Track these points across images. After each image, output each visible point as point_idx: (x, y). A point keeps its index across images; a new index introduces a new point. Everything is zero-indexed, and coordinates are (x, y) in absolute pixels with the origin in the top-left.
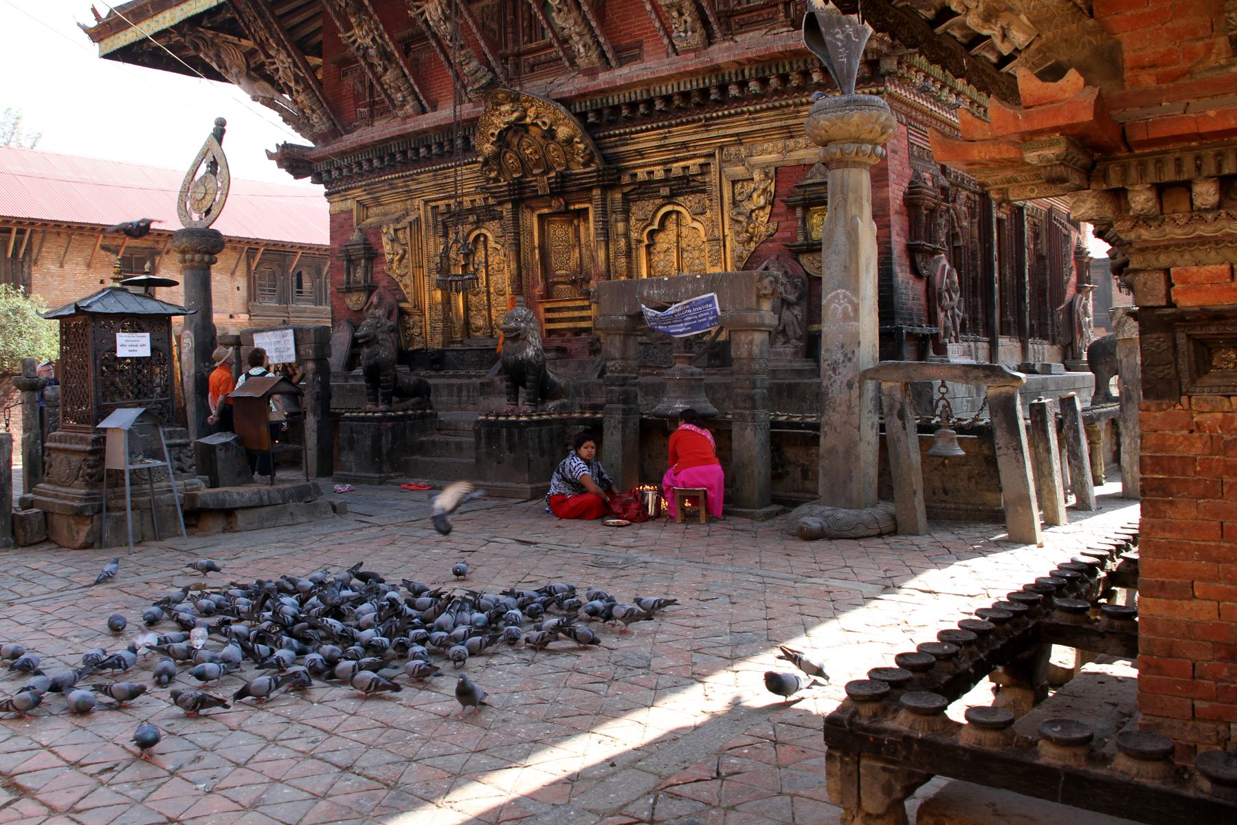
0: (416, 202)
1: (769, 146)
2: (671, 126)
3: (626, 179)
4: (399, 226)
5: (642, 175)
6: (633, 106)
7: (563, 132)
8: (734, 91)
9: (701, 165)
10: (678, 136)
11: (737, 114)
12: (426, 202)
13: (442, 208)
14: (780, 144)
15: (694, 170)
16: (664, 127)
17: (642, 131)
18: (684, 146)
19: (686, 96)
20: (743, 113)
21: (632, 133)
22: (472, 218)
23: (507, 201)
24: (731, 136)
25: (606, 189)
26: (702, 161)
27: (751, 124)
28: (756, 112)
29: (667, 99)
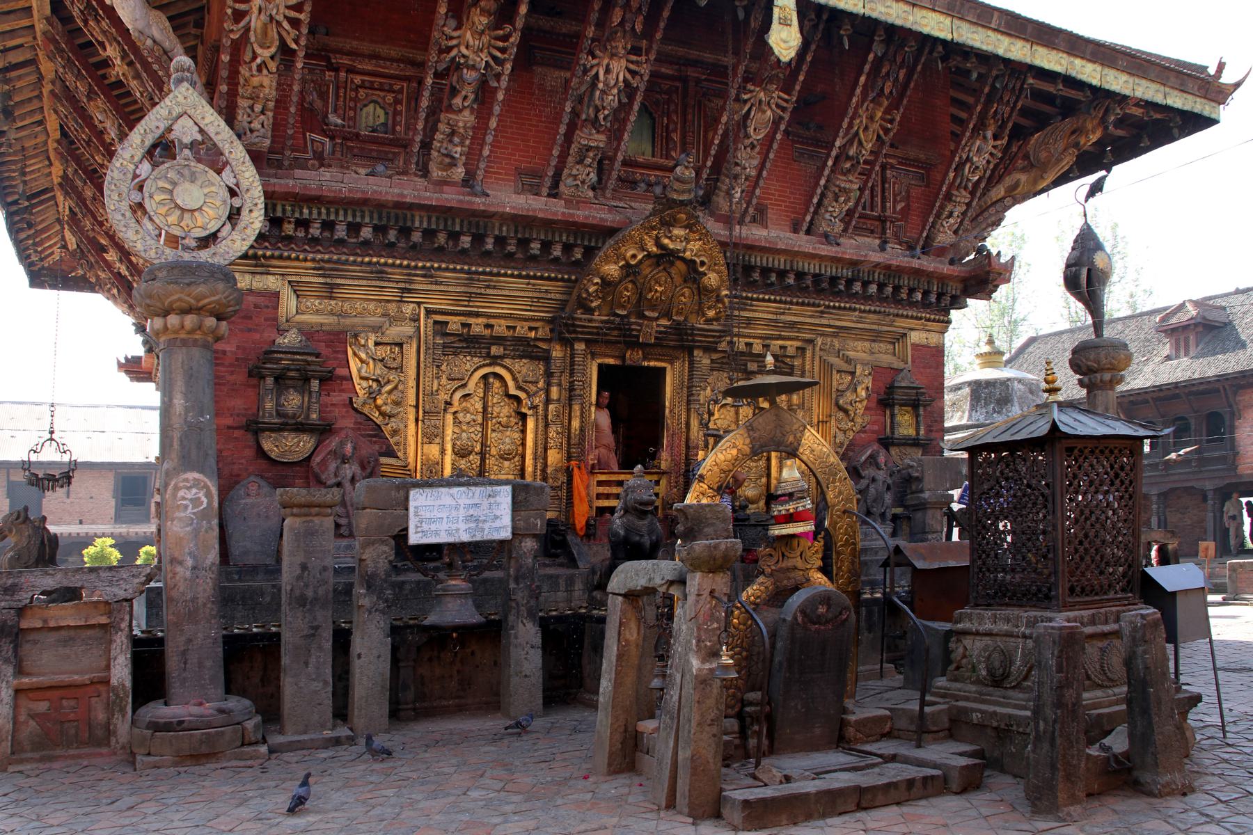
0: (408, 309)
1: (859, 345)
2: (791, 303)
3: (723, 346)
4: (386, 340)
5: (741, 344)
6: (765, 271)
7: (712, 279)
8: (857, 287)
9: (798, 348)
10: (795, 315)
11: (850, 309)
12: (429, 312)
13: (454, 324)
14: (867, 344)
15: (791, 351)
16: (785, 303)
17: (764, 300)
18: (792, 325)
19: (817, 277)
20: (855, 310)
21: (752, 299)
22: (495, 350)
23: (580, 340)
24: (837, 327)
25: (708, 349)
26: (799, 344)
27: (858, 322)
28: (864, 311)
29: (800, 275)
